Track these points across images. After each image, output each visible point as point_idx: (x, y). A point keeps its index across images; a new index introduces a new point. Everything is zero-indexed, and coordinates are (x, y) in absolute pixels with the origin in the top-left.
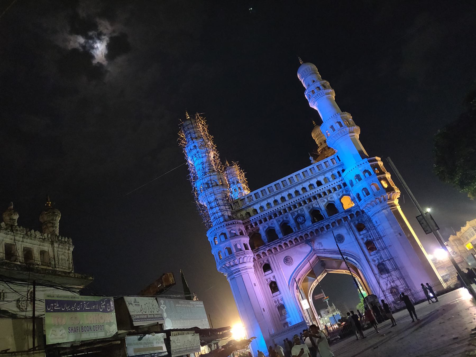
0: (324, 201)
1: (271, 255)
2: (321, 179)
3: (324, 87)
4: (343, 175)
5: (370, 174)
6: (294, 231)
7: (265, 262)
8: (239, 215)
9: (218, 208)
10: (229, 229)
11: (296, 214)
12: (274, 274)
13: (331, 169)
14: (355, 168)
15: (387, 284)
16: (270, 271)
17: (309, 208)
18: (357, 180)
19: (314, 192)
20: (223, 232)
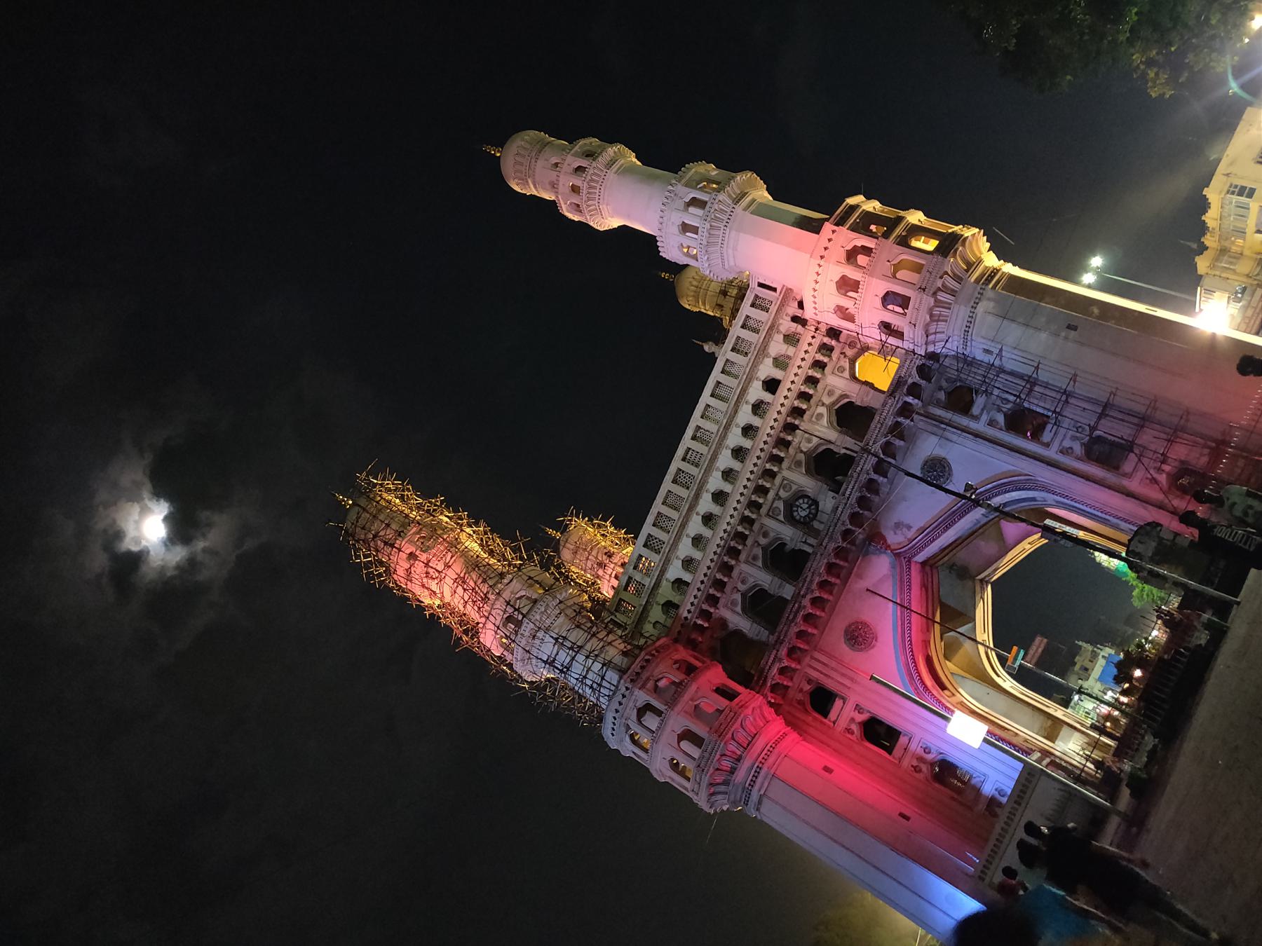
0: (820, 416)
1: (807, 660)
2: (767, 370)
3: (590, 155)
4: (808, 314)
5: (867, 251)
6: (809, 550)
7: (807, 687)
8: (648, 628)
9: (581, 658)
10: (650, 685)
12: (852, 700)
13: (771, 328)
15: (1154, 481)
16: (838, 703)
17: (798, 464)
18: (851, 294)
19: (776, 416)
20: (640, 704)
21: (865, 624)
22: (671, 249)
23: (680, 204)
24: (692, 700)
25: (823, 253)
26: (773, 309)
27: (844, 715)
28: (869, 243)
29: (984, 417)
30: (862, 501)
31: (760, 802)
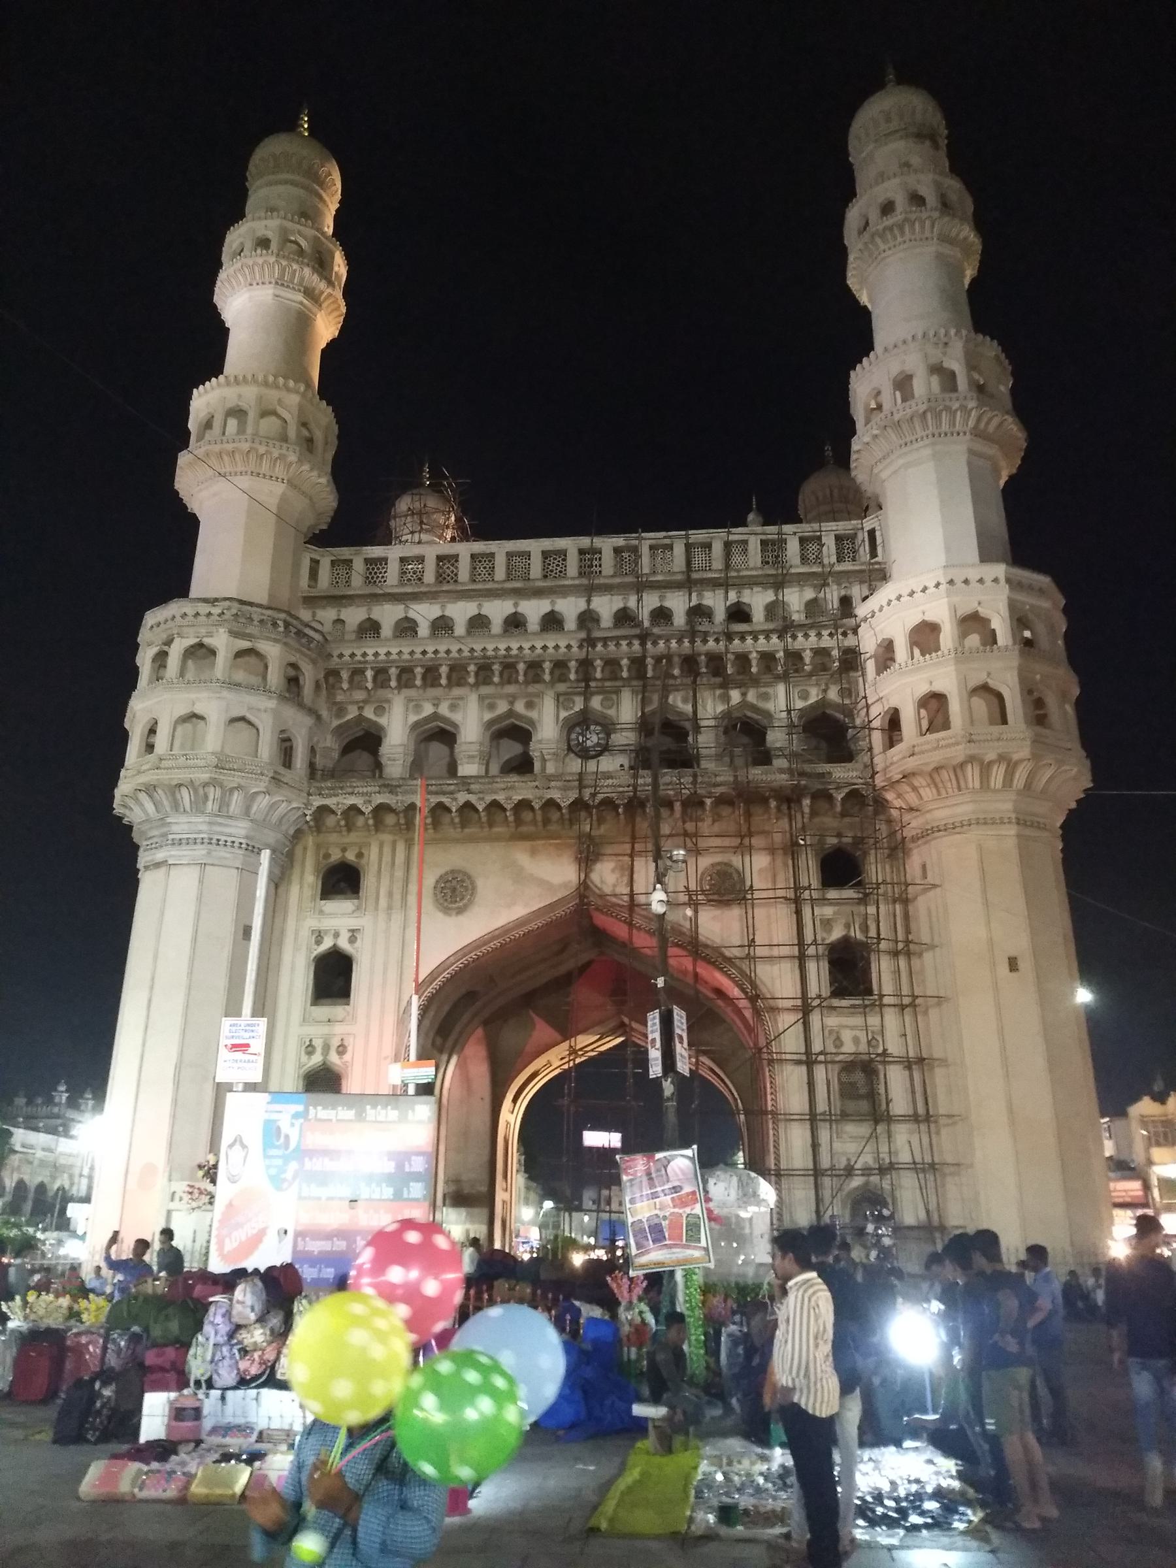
0: (726, 698)
1: (387, 837)
3: (945, 206)
5: (991, 638)
7: (351, 856)
11: (579, 704)
14: (932, 590)
18: (917, 652)
20: (206, 641)
21: (474, 888)
22: (867, 383)
23: (935, 355)
24: (250, 709)
25: (958, 581)
26: (847, 566)
27: (339, 920)
28: (1004, 637)
29: (828, 911)
30: (635, 805)
31: (158, 865)
